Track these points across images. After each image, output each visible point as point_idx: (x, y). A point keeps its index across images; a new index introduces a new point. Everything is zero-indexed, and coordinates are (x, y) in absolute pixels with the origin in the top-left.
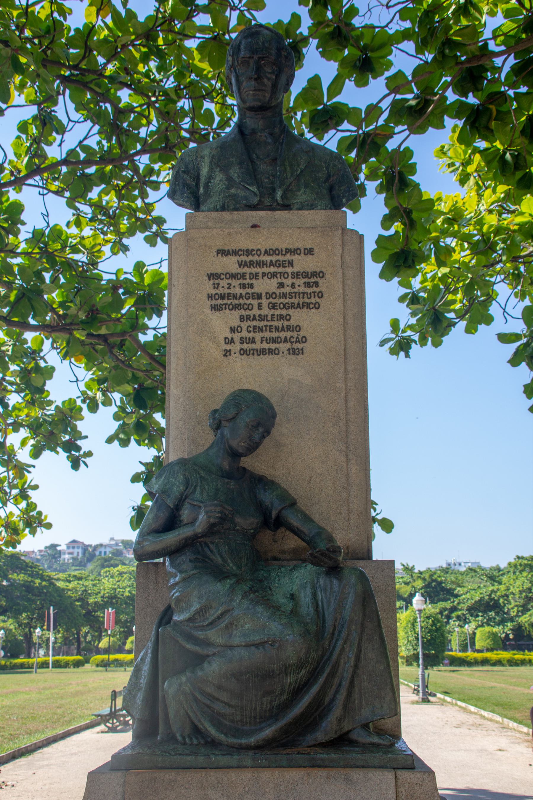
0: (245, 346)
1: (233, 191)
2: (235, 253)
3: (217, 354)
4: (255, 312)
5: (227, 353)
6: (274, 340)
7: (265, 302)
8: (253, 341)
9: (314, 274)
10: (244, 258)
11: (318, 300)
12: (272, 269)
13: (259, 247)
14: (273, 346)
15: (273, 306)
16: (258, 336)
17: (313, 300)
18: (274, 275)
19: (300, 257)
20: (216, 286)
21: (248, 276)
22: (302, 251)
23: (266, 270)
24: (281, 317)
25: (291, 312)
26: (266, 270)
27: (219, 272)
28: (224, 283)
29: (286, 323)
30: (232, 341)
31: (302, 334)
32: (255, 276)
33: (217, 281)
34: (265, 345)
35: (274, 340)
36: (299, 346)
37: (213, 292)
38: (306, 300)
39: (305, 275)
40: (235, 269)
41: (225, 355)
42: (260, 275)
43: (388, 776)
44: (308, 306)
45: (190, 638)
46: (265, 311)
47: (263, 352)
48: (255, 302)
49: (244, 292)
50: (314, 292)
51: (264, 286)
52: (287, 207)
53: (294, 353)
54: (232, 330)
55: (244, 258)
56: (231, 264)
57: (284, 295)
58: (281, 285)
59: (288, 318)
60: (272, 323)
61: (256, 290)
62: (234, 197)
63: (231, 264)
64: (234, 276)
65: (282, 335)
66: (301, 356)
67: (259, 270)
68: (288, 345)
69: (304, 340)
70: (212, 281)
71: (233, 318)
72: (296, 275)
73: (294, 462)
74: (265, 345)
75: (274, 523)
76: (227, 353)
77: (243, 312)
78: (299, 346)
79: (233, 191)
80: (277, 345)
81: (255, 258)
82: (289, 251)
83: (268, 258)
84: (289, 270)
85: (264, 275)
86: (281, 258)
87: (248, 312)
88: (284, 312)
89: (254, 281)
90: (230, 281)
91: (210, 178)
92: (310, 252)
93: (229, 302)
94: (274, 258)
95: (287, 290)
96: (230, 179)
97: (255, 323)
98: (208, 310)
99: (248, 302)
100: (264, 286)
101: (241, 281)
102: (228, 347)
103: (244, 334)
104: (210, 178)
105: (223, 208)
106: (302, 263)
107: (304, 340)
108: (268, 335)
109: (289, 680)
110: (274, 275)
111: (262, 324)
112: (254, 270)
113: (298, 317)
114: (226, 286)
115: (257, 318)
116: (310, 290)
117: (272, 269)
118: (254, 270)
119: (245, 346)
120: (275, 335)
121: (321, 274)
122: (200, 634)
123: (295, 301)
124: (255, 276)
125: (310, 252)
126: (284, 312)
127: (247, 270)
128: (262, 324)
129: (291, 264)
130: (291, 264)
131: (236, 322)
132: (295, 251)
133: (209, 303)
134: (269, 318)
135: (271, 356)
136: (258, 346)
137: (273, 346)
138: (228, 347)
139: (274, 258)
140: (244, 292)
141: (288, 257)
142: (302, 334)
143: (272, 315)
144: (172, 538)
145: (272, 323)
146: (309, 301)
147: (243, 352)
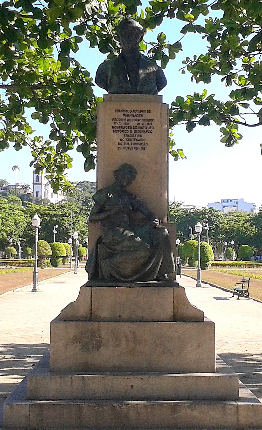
0: (126, 146)
1: (121, 85)
2: (122, 111)
3: (115, 148)
4: (129, 133)
5: (119, 148)
6: (136, 144)
7: (132, 129)
8: (129, 144)
9: (151, 120)
10: (126, 113)
11: (152, 130)
12: (135, 118)
13: (131, 109)
14: (136, 146)
15: (135, 131)
16: (130, 142)
17: (150, 130)
18: (136, 120)
19: (145, 113)
20: (115, 123)
21: (127, 120)
22: (147, 111)
23: (133, 118)
24: (139, 136)
25: (142, 134)
26: (133, 118)
27: (117, 118)
28: (118, 122)
29: (140, 138)
30: (121, 144)
31: (146, 142)
32: (129, 120)
33: (115, 122)
34: (132, 146)
35: (136, 144)
36: (145, 146)
37: (114, 125)
38: (147, 130)
39: (148, 120)
40: (122, 117)
41: (119, 149)
42: (131, 120)
43: (171, 289)
44: (148, 132)
45: (109, 248)
46: (133, 133)
47: (132, 148)
48: (129, 130)
49: (125, 126)
50: (151, 127)
51: (133, 124)
52: (141, 93)
53: (143, 149)
54: (121, 140)
55: (126, 113)
56: (121, 115)
57: (140, 128)
58: (139, 124)
59: (141, 136)
60: (135, 138)
61: (130, 125)
62: (121, 87)
63: (121, 115)
64: (122, 120)
65: (139, 142)
66: (145, 150)
67: (131, 118)
68: (141, 146)
69: (147, 144)
70: (114, 121)
71: (121, 135)
72: (144, 120)
73: (142, 185)
74: (132, 146)
75: (136, 210)
76: (119, 148)
77: (125, 133)
78: (145, 146)
79: (121, 85)
80: (137, 146)
81: (129, 113)
82: (142, 111)
83: (134, 114)
84: (142, 118)
85: (133, 119)
86: (139, 113)
87: (127, 134)
88: (139, 134)
89: (129, 122)
90: (120, 122)
91: (111, 78)
92: (149, 111)
93: (120, 129)
94: (136, 114)
95: (141, 126)
96: (119, 79)
97: (129, 138)
98: (112, 132)
99: (127, 129)
100: (133, 124)
101: (124, 122)
102: (120, 146)
103: (125, 141)
104: (111, 78)
105: (117, 92)
106: (146, 116)
107: (147, 144)
108: (134, 142)
109: (142, 261)
110: (136, 120)
111: (131, 138)
112: (128, 118)
113: (145, 136)
114: (119, 123)
115: (130, 136)
116: (149, 126)
117: (135, 118)
118: (128, 118)
119: (126, 146)
120: (137, 142)
121: (153, 120)
122: (113, 247)
123: (144, 130)
124: (129, 120)
125: (149, 111)
126: (139, 134)
127: (126, 118)
128: (131, 138)
129: (142, 116)
130: (142, 116)
131: (122, 137)
132: (145, 111)
133: (113, 129)
134: (134, 136)
135: (135, 150)
136: (131, 146)
137: (136, 146)
138: (120, 146)
139: (136, 114)
140: (125, 126)
141: (141, 113)
142: (146, 142)
143: (135, 135)
144: (102, 216)
145: (135, 138)
146: (149, 130)
147: (125, 148)
